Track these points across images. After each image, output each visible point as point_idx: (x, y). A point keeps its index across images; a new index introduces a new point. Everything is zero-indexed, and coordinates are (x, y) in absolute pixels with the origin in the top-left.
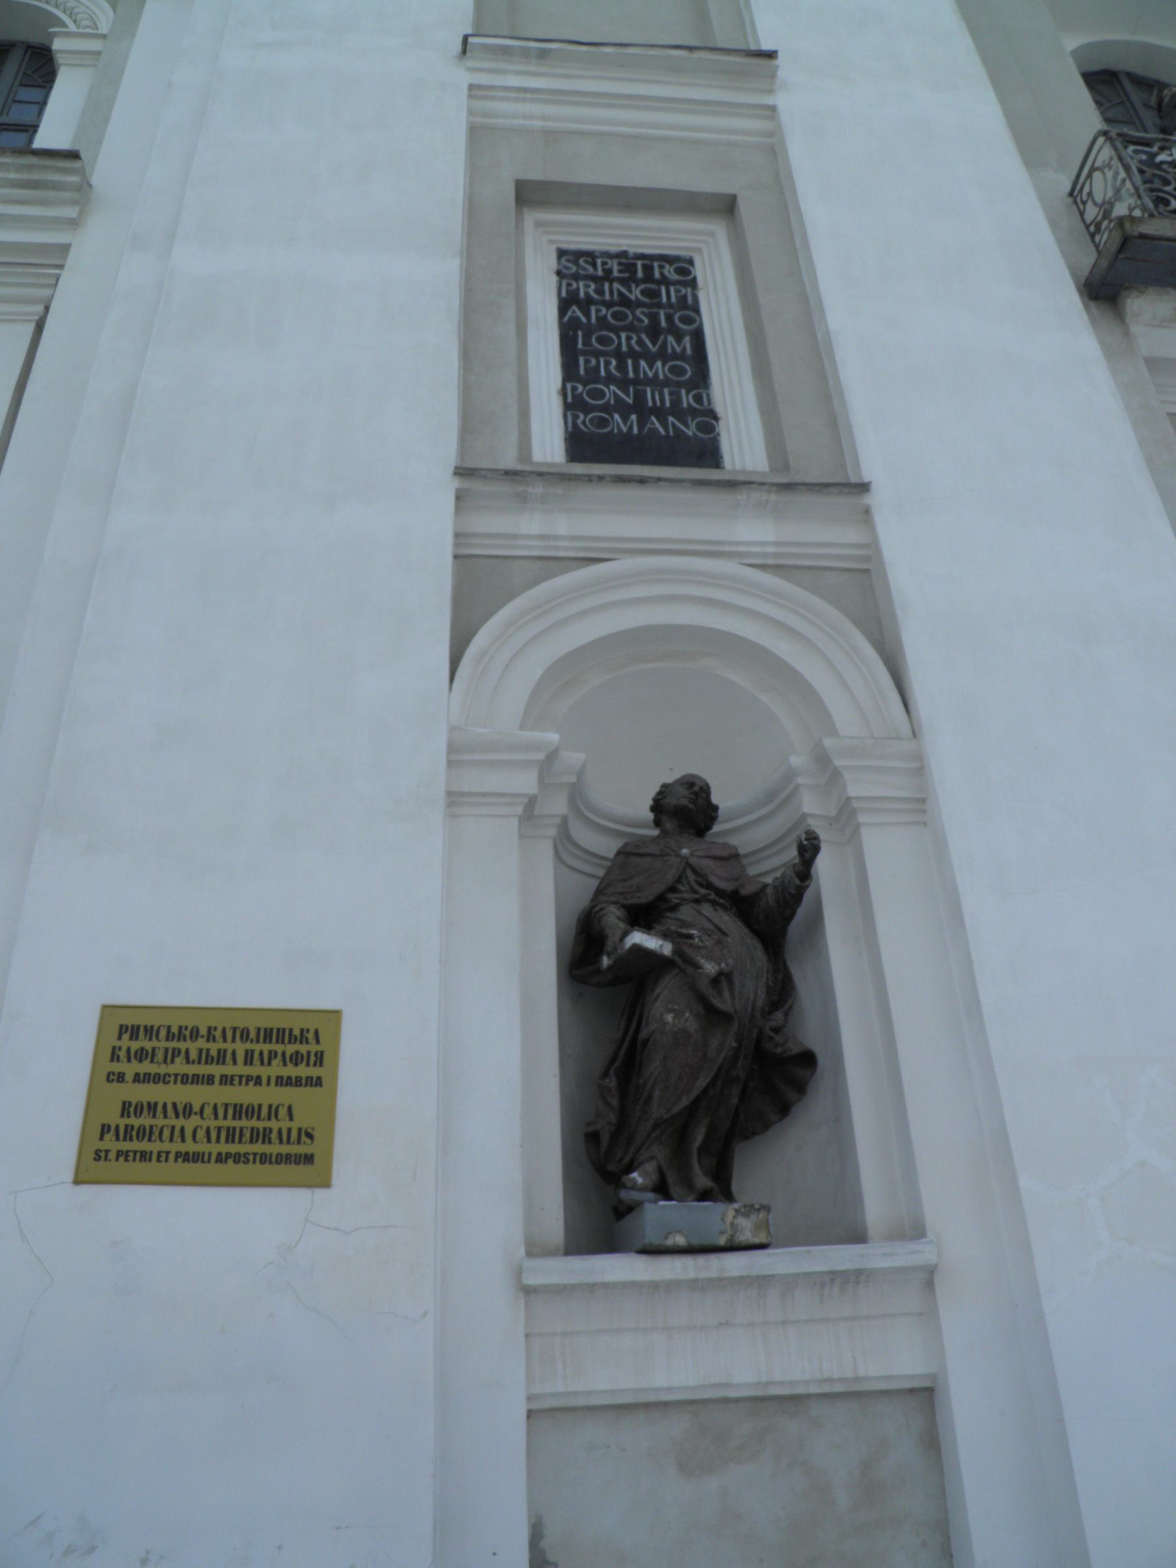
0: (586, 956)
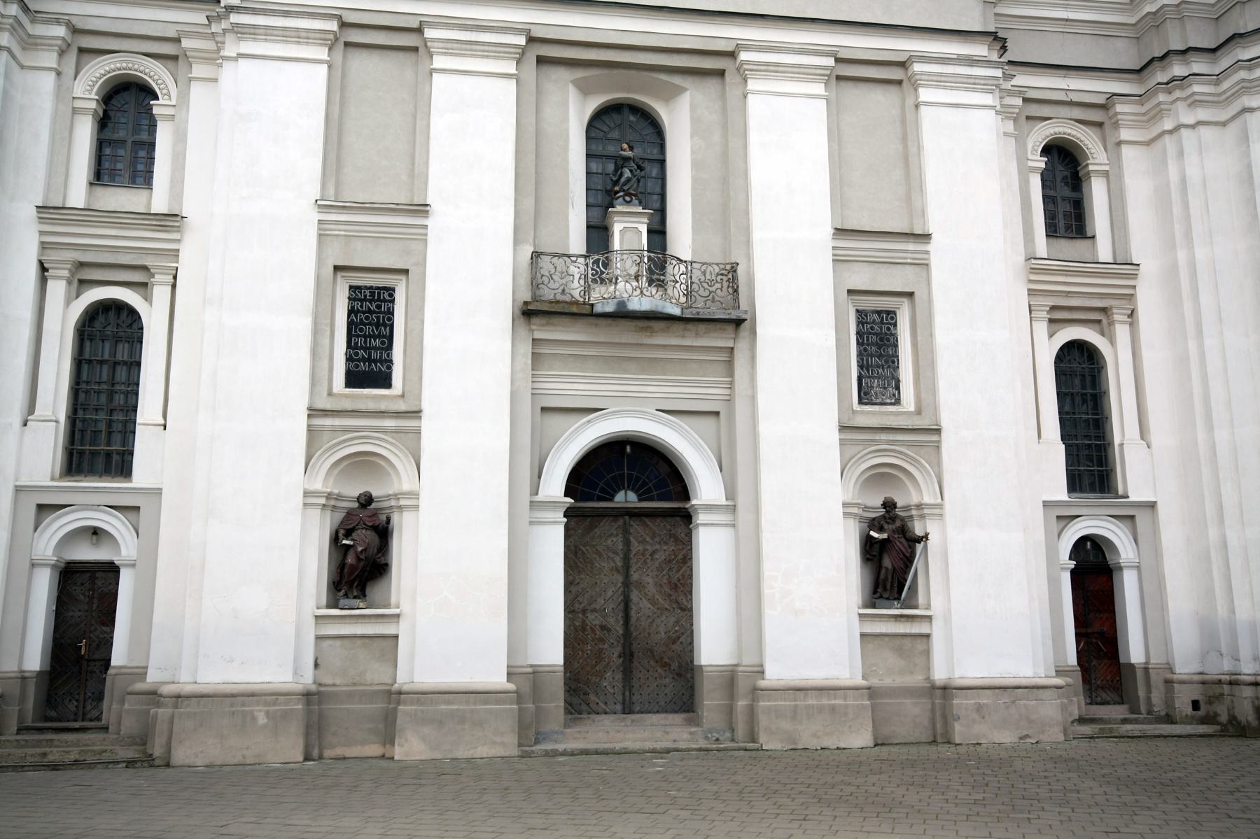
0: (335, 539)
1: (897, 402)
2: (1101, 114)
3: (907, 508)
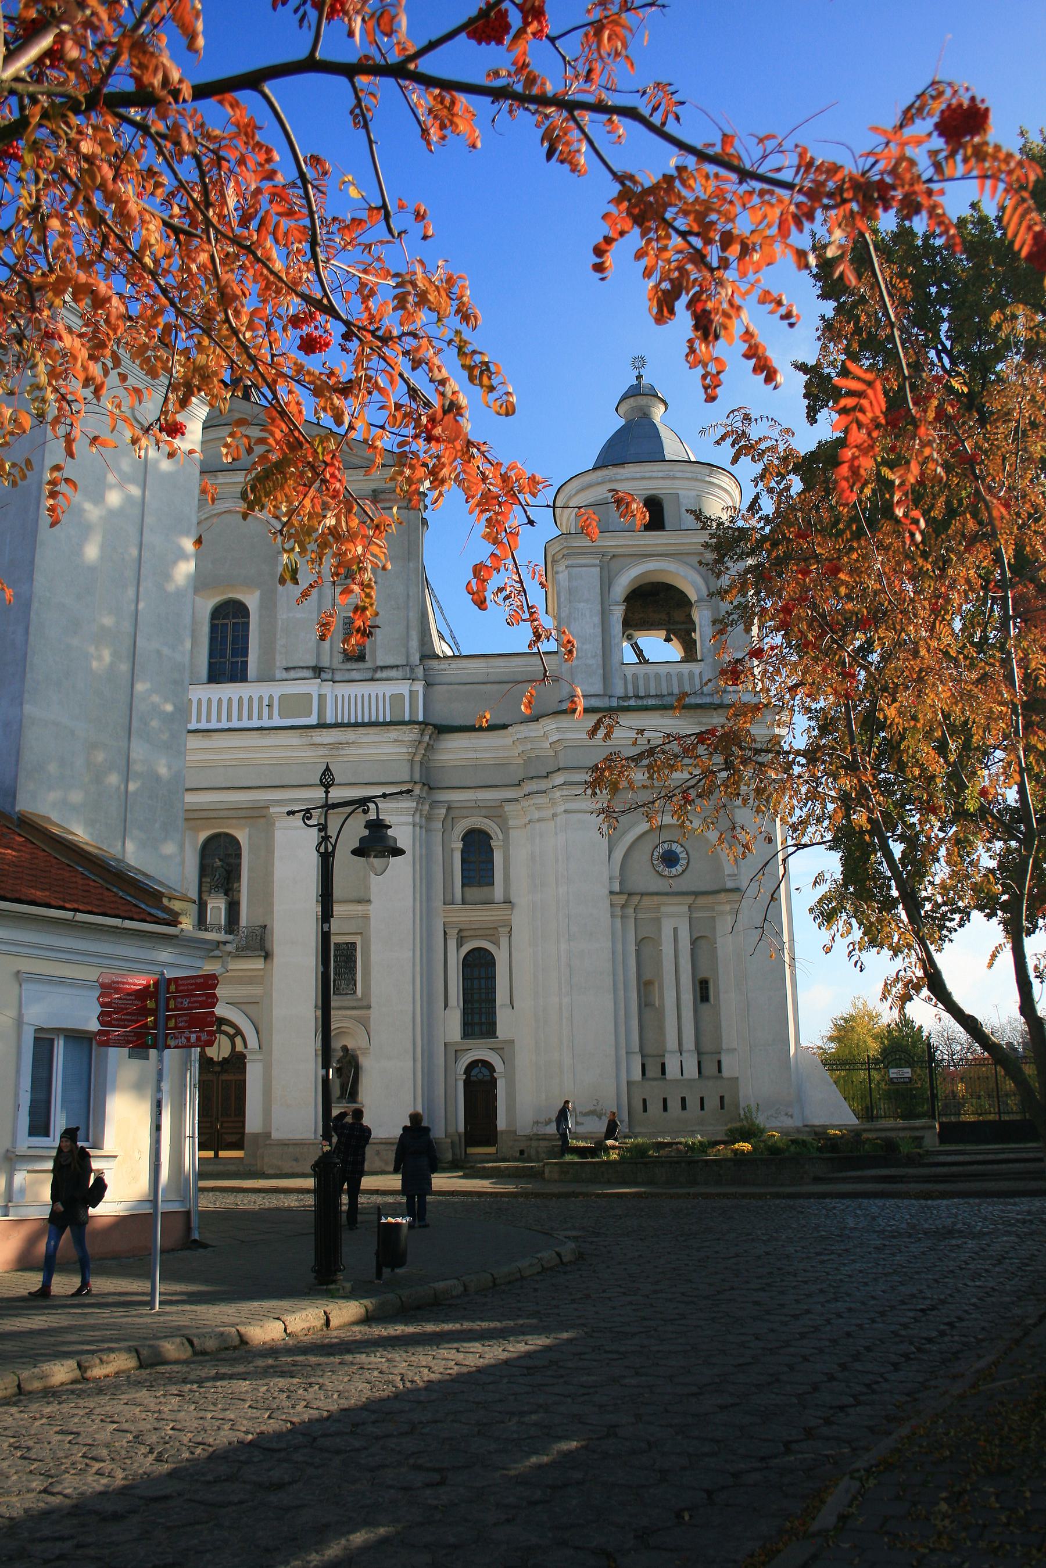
1: (355, 992)
2: (496, 812)
3: (354, 1050)
